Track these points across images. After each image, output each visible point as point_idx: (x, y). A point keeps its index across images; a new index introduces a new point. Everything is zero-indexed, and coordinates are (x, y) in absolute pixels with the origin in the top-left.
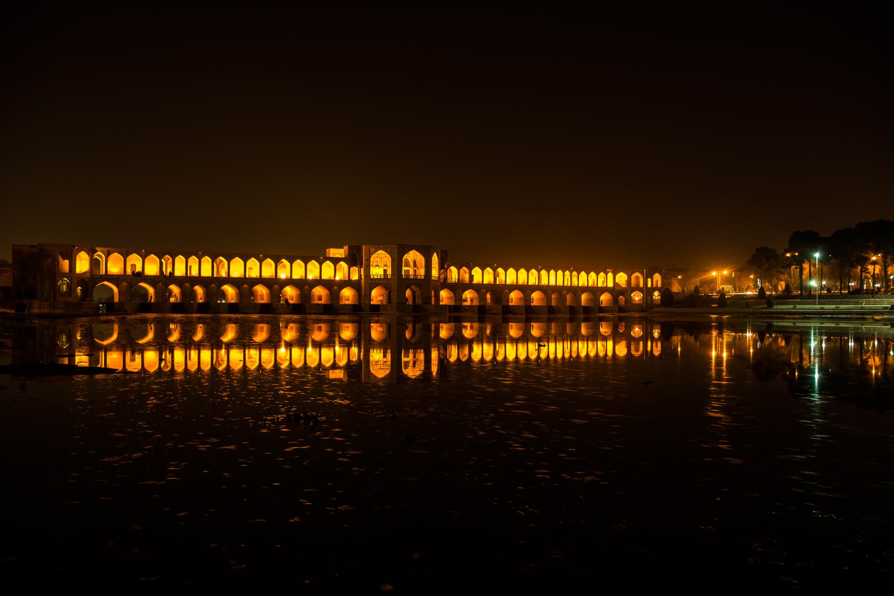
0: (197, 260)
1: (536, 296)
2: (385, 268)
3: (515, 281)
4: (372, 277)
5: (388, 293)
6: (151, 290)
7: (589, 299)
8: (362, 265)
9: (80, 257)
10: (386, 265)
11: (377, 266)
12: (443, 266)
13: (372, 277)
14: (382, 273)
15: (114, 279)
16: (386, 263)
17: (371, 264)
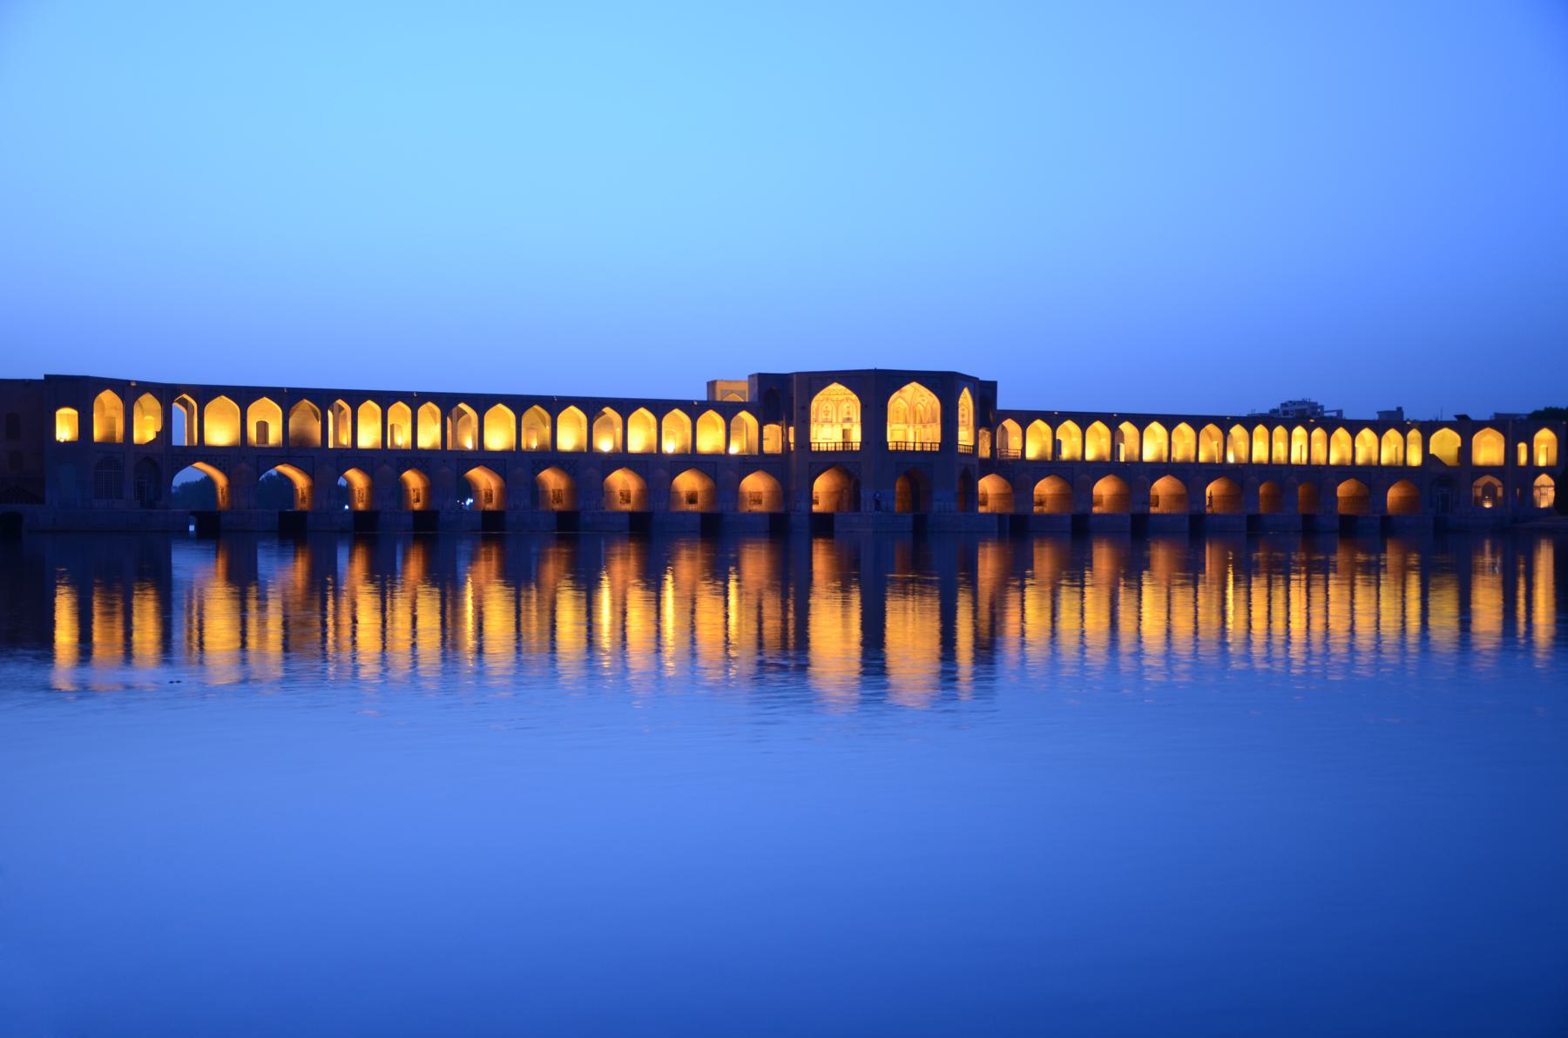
0: (408, 410)
1: (1104, 488)
2: (847, 426)
3: (1165, 454)
4: (814, 447)
6: (300, 480)
7: (997, 494)
8: (792, 419)
9: (141, 405)
10: (848, 420)
11: (826, 421)
13: (814, 447)
14: (840, 439)
15: (216, 456)
16: (848, 413)
17: (813, 416)
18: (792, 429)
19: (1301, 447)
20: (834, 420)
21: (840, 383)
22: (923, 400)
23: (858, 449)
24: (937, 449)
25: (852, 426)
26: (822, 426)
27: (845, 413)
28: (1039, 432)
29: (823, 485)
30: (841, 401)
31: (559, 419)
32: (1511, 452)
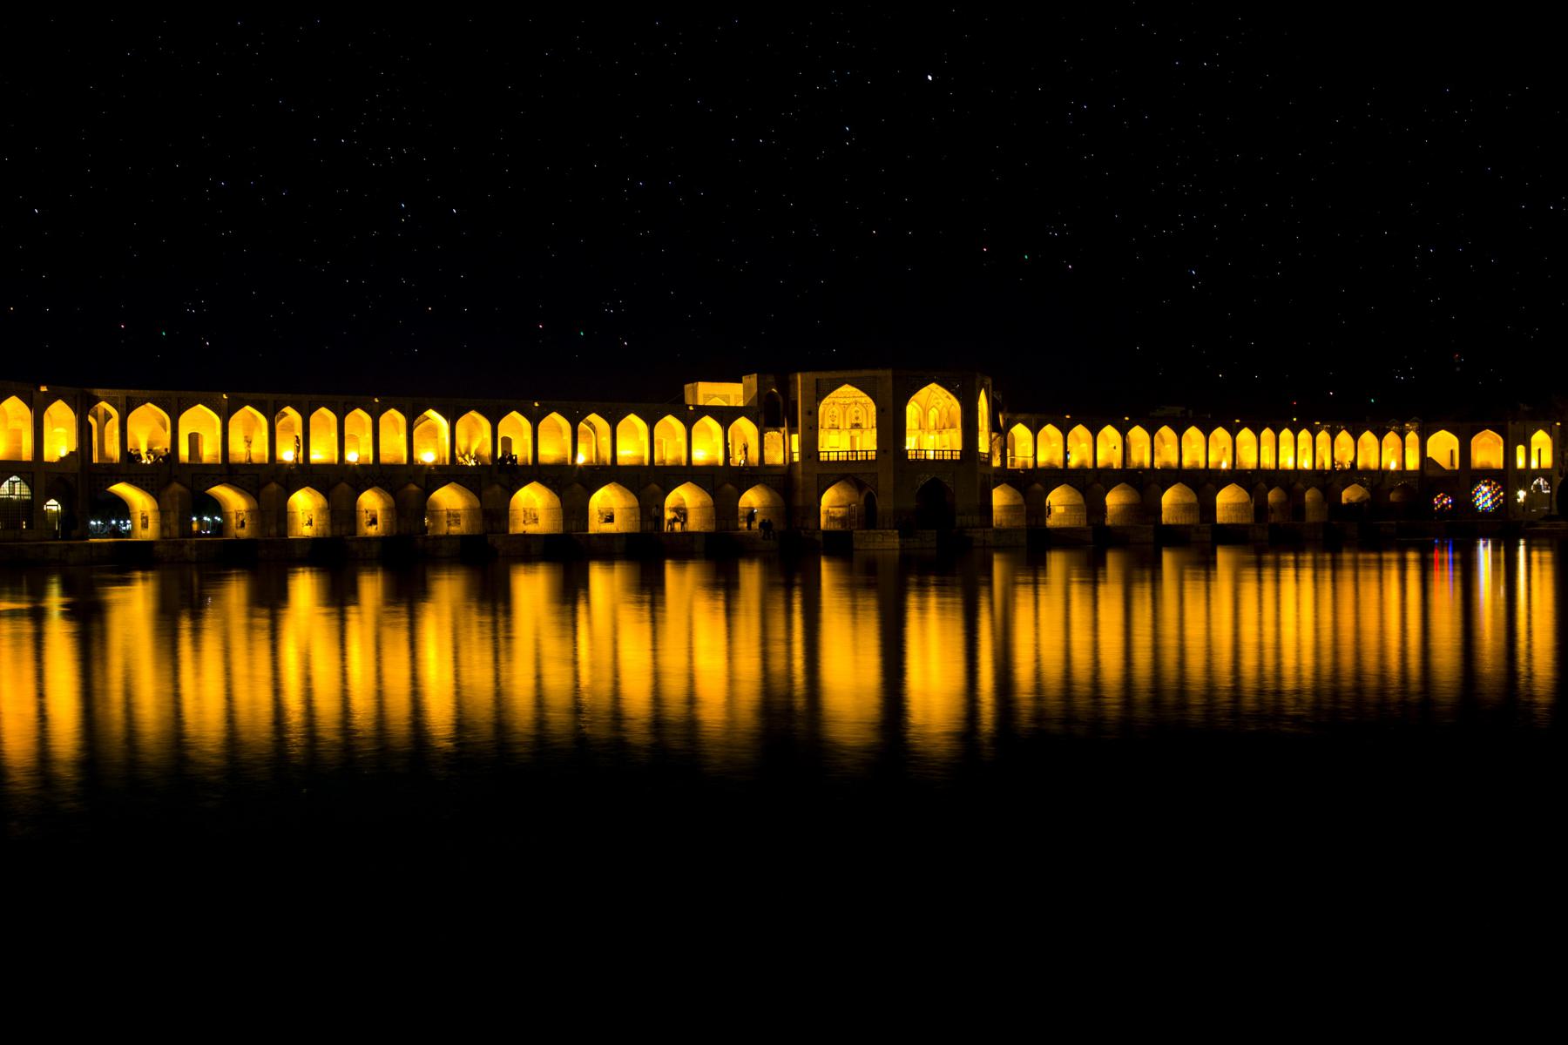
0: (367, 418)
5: (866, 499)
8: (796, 424)
9: (49, 415)
10: (857, 426)
11: (832, 427)
12: (1000, 431)
13: (823, 457)
16: (857, 418)
17: (820, 423)
18: (795, 438)
19: (1224, 449)
20: (841, 427)
21: (853, 385)
22: (938, 403)
23: (874, 458)
24: (958, 458)
25: (862, 433)
26: (829, 433)
27: (854, 417)
28: (1049, 439)
29: (830, 500)
30: (850, 404)
31: (540, 427)
32: (1509, 455)
